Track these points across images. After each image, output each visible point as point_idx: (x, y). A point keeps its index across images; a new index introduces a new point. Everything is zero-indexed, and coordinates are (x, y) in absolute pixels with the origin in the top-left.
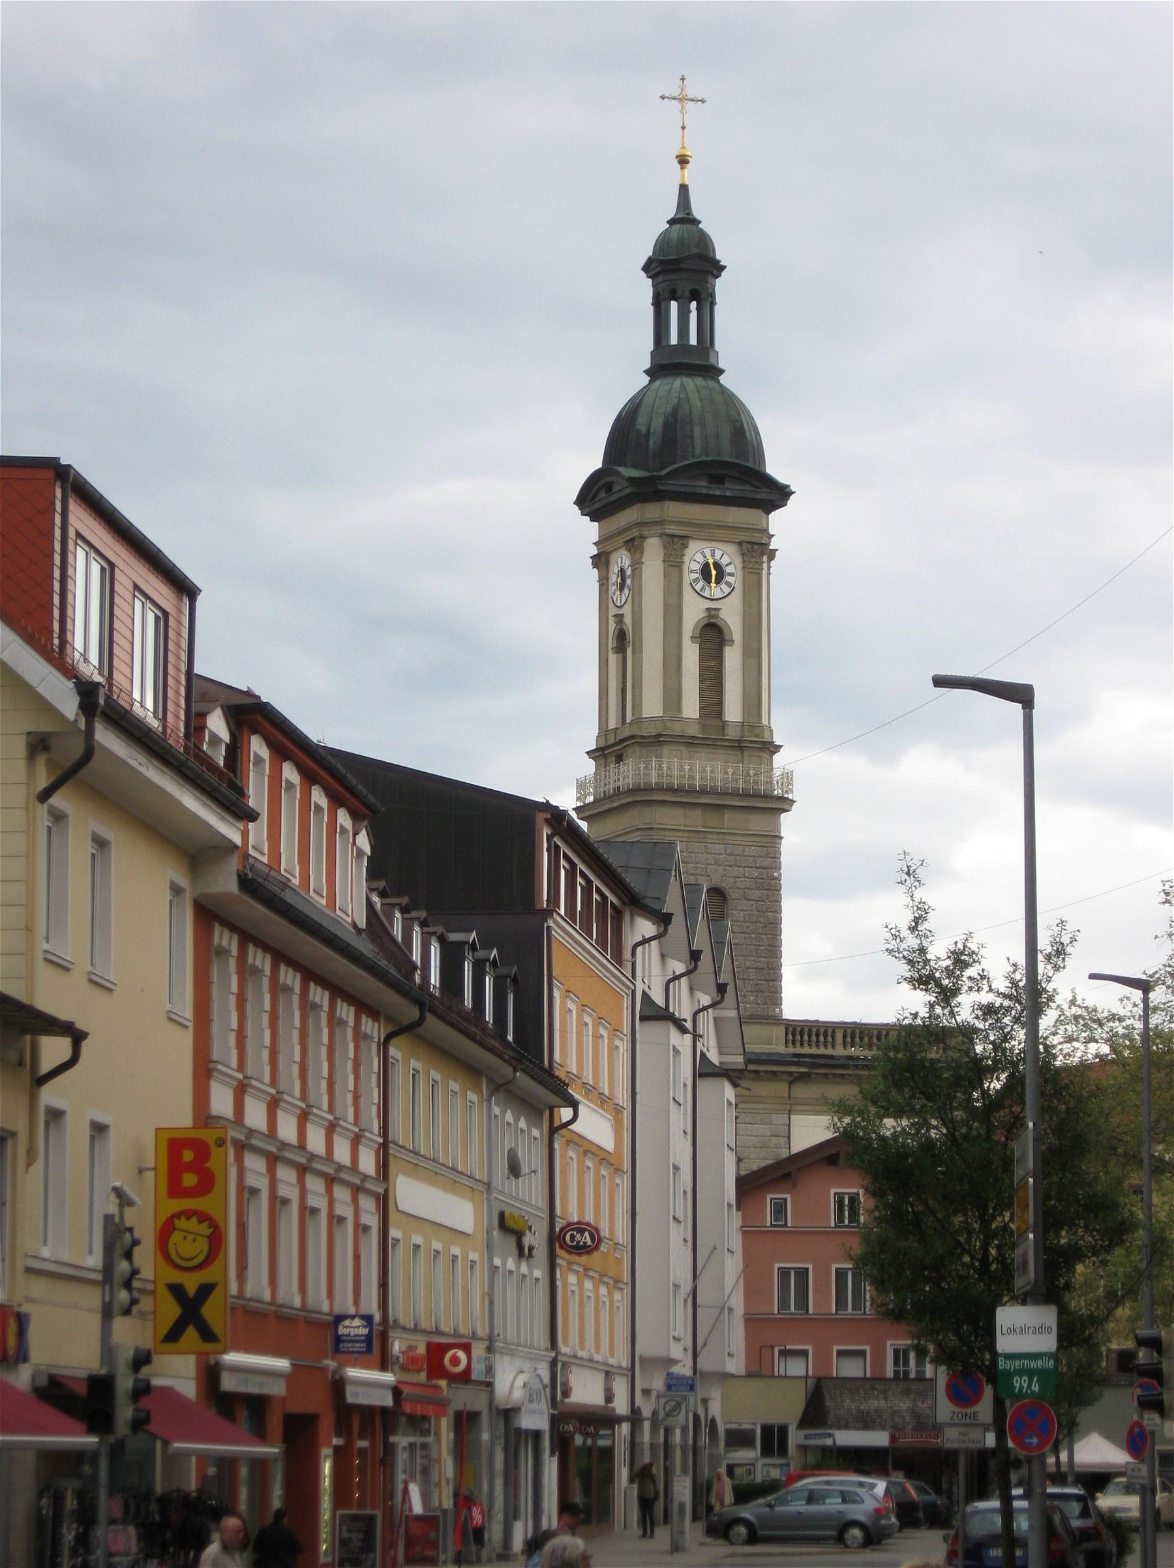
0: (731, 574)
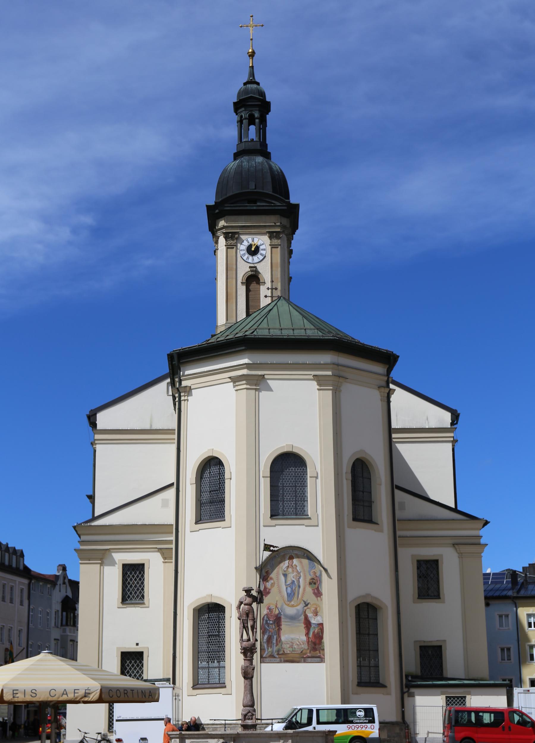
0: (262, 250)
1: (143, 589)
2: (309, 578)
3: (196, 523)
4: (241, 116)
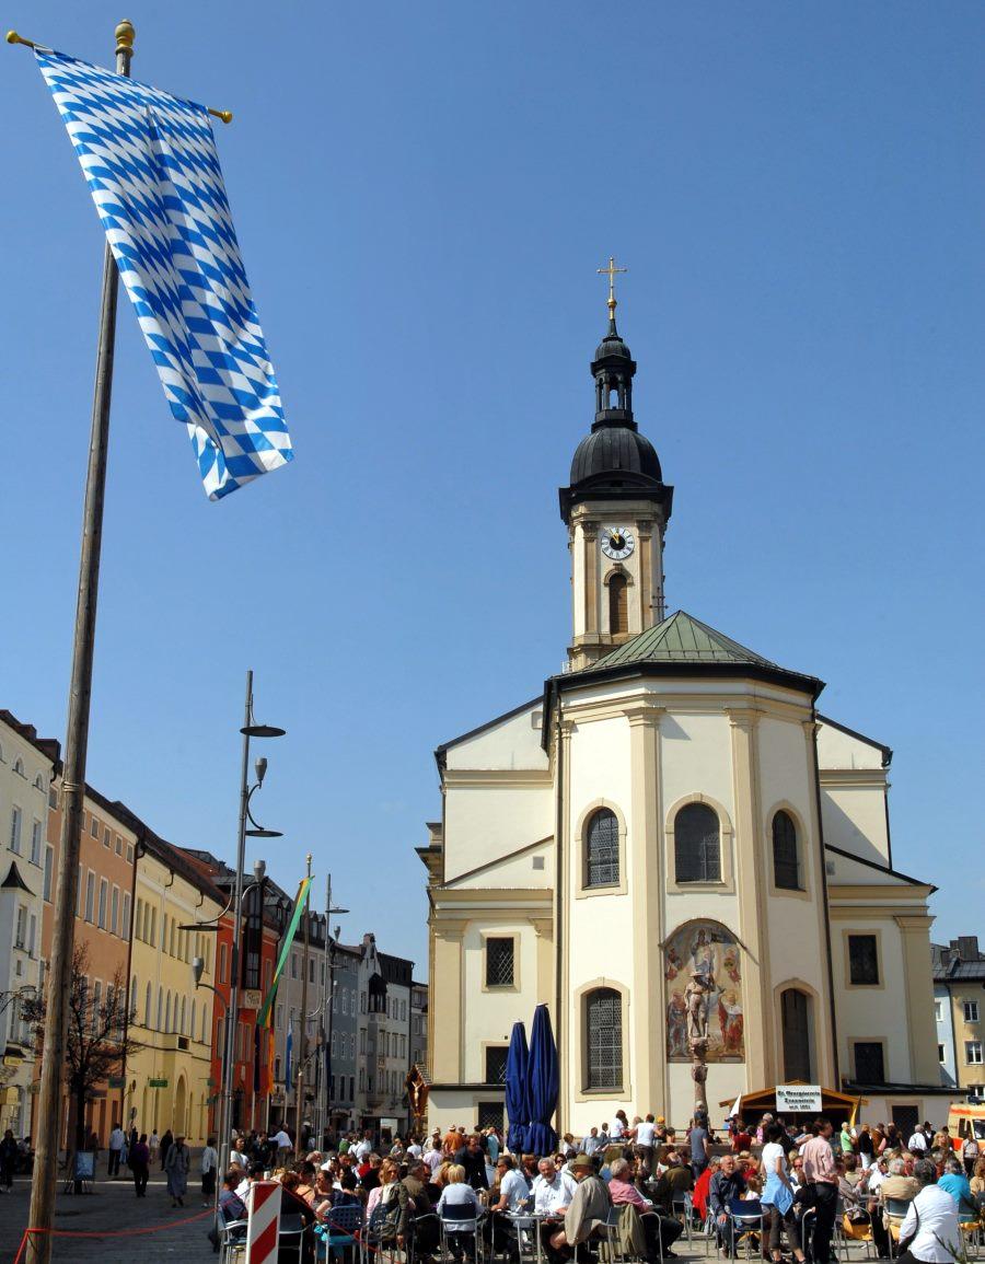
1: (512, 970)
2: (723, 961)
3: (583, 888)
4: (601, 379)
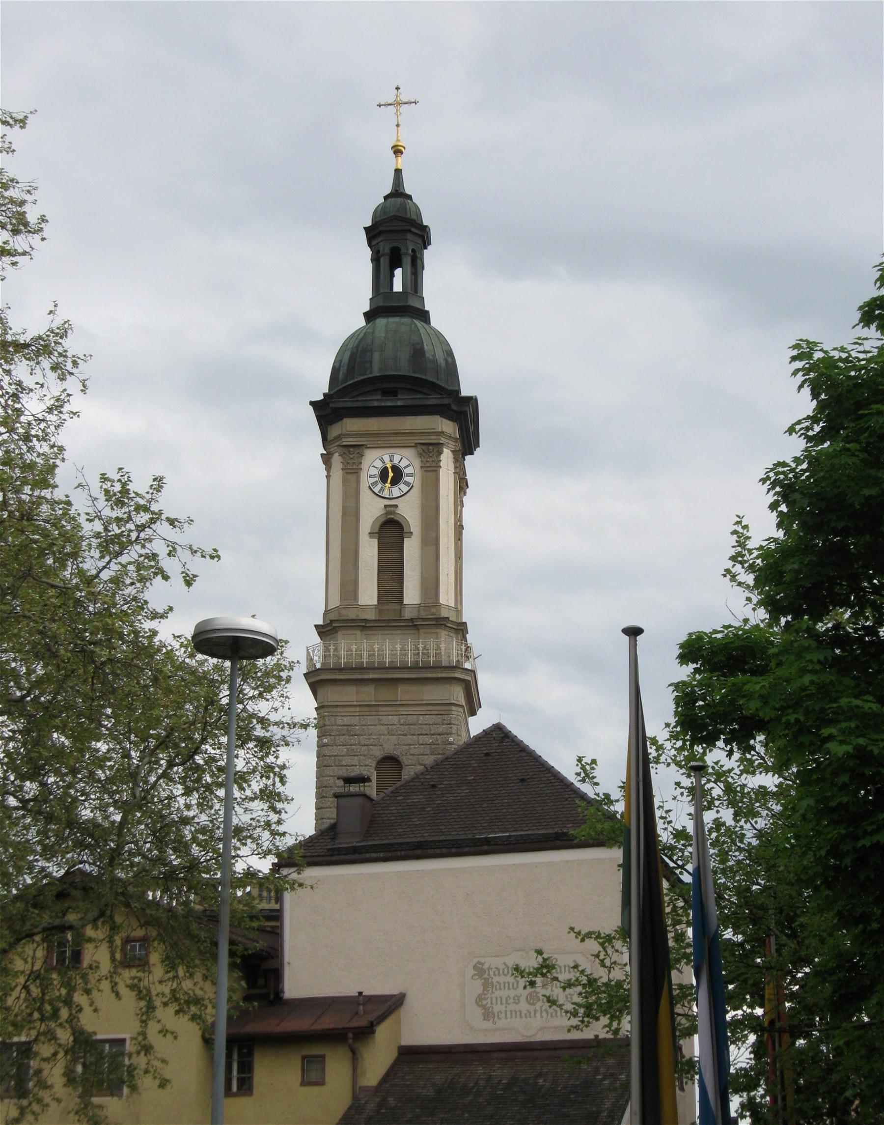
0: (408, 475)
